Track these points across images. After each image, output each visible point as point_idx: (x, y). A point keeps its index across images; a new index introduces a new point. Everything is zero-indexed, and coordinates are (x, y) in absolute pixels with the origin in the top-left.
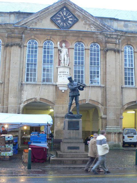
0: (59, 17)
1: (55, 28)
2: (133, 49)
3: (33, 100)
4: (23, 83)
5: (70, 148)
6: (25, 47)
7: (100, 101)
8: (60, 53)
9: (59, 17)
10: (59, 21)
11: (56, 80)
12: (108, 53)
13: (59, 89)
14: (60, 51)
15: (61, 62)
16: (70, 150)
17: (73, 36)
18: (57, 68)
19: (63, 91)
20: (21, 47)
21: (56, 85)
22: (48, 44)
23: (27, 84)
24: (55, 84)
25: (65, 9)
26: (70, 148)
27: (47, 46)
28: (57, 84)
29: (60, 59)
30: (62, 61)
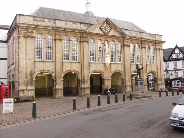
0: (103, 27)
1: (102, 33)
2: (69, 39)
3: (69, 72)
5: (141, 92)
7: (122, 71)
9: (103, 27)
10: (104, 29)
11: (104, 60)
12: (57, 41)
16: (142, 93)
19: (108, 66)
23: (92, 63)
25: (105, 23)
26: (141, 92)
28: (105, 62)
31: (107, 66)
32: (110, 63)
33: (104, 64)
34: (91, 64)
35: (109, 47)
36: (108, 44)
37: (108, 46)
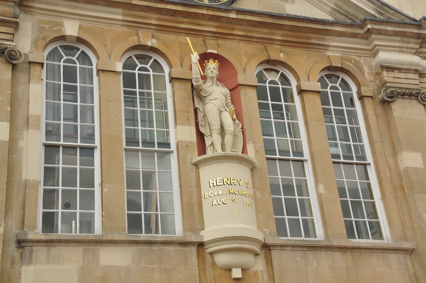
4: (31, 236)
6: (36, 70)
8: (197, 106)
13: (214, 264)
14: (196, 93)
15: (208, 143)
17: (248, 39)
18: (196, 165)
19: (237, 273)
20: (14, 66)
21: (201, 245)
22: (139, 66)
24: (194, 239)
27: (137, 72)
28: (207, 235)
29: (202, 130)
30: (213, 138)
31: (230, 270)
32: (267, 247)
33: (194, 250)
34: (41, 252)
35: (238, 115)
36: (234, 90)
37: (235, 100)
